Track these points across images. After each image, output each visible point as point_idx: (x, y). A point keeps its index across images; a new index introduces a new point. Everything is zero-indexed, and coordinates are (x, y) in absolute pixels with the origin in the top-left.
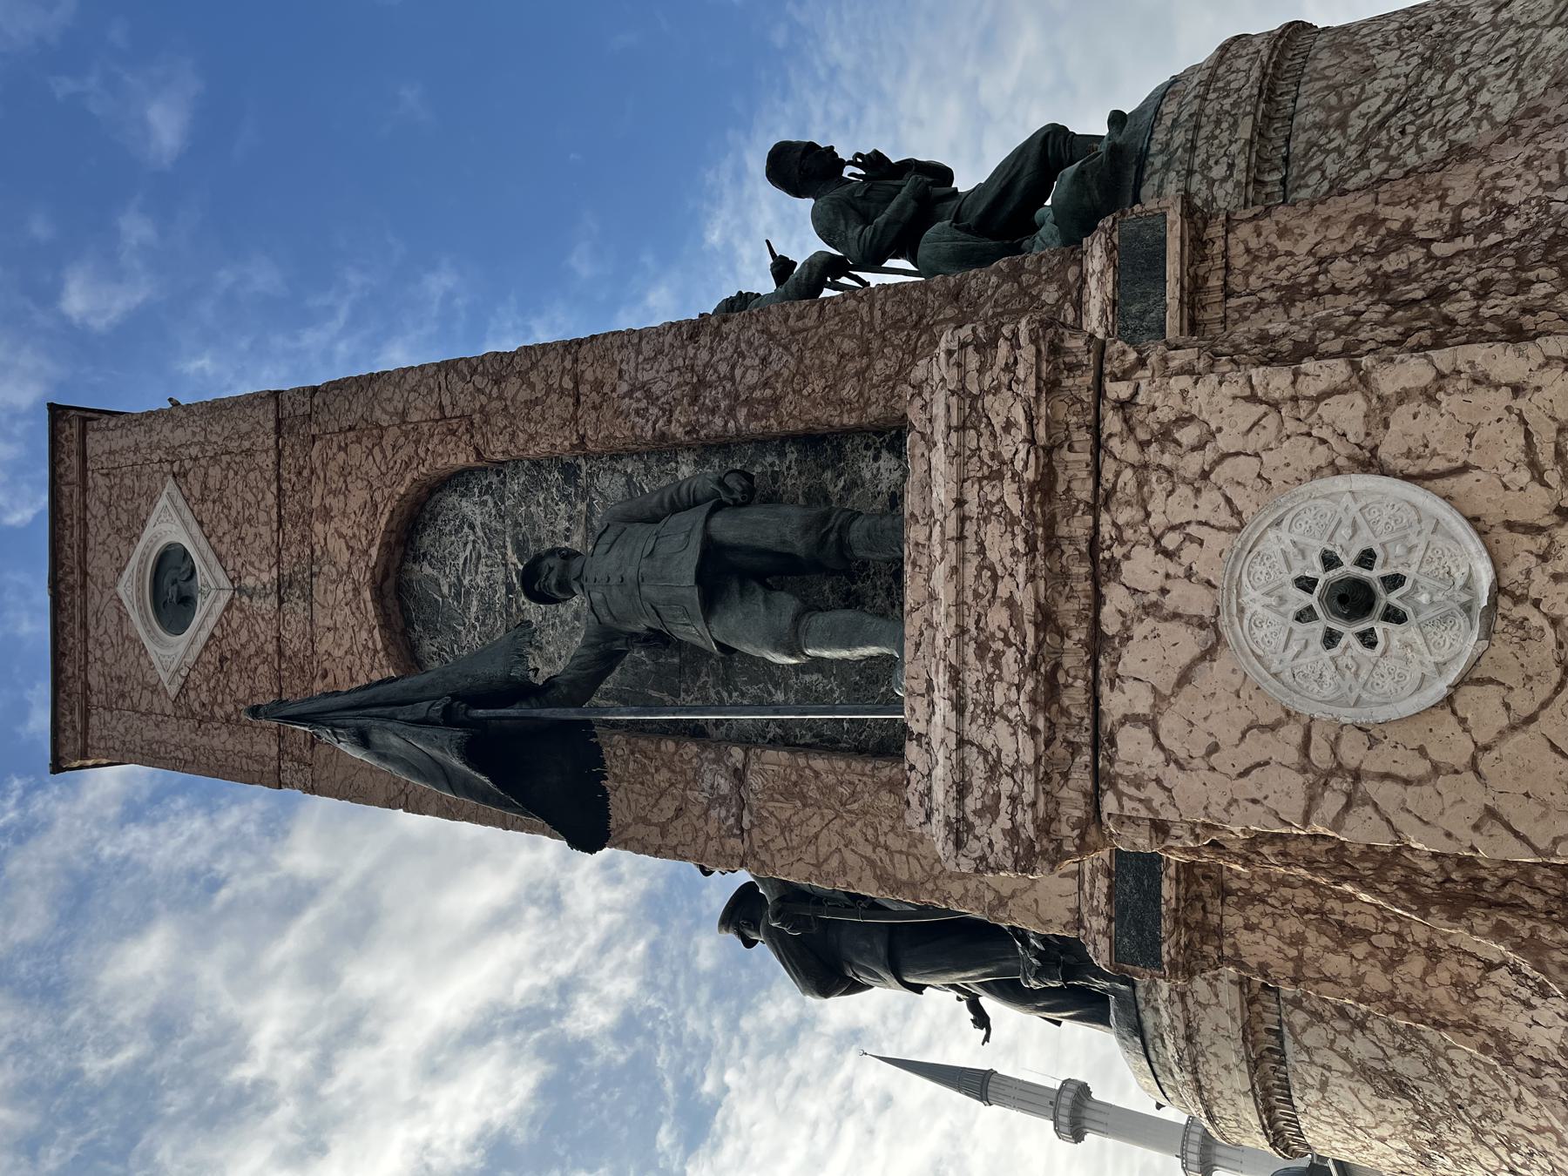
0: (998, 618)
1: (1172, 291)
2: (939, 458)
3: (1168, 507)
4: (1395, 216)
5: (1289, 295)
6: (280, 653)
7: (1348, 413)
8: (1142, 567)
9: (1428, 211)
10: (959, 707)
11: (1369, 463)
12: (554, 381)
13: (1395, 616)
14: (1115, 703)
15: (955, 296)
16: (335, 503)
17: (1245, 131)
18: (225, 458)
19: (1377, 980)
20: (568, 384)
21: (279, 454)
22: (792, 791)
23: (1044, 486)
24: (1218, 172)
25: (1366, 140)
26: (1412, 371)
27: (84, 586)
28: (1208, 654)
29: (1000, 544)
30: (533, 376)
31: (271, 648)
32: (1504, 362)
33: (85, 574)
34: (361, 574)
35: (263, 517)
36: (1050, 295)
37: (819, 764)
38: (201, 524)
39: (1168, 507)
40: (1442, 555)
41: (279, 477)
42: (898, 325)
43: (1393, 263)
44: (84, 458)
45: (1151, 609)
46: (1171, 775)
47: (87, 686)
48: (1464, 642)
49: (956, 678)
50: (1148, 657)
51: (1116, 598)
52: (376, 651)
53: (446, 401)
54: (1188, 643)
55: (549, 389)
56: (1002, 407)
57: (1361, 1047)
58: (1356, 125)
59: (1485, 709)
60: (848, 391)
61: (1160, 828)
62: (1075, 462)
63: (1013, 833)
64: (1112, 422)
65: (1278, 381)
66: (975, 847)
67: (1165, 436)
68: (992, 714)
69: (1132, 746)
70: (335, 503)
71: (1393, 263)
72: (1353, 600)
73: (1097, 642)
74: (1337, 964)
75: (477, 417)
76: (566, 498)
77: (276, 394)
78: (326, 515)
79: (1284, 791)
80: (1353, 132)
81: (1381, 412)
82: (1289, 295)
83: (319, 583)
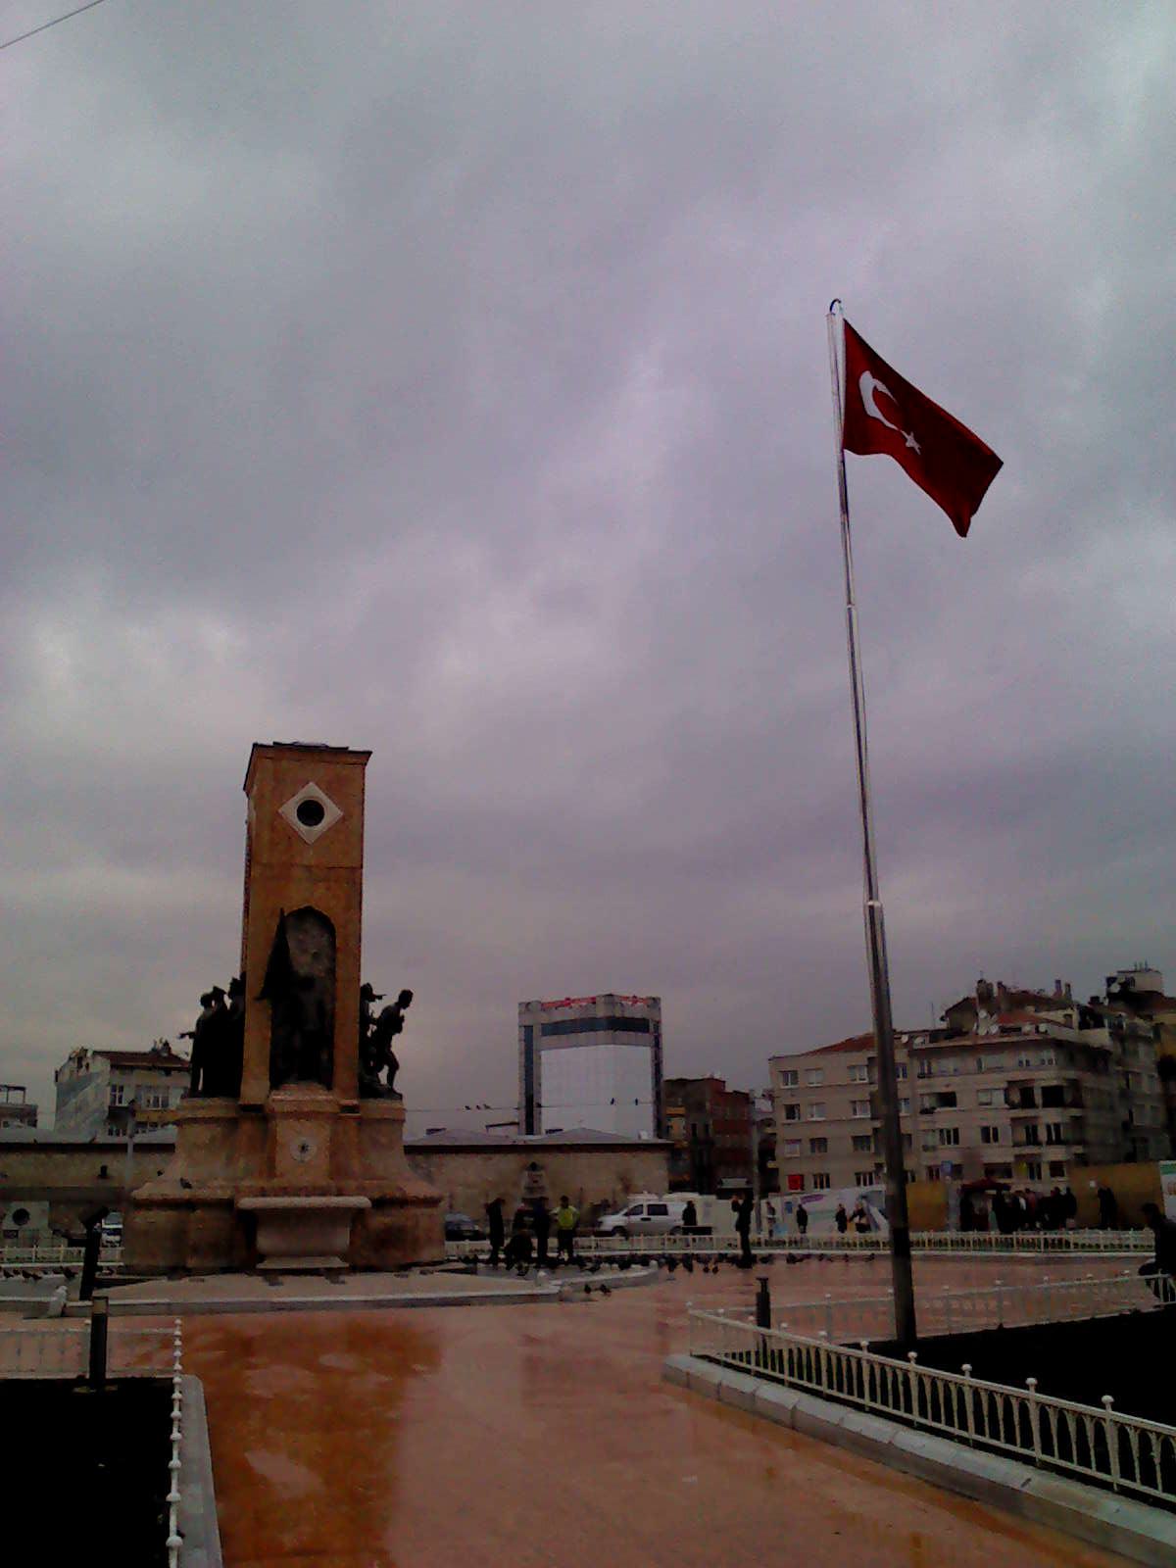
2: (324, 1097)
40: (307, 1157)
77: (362, 867)
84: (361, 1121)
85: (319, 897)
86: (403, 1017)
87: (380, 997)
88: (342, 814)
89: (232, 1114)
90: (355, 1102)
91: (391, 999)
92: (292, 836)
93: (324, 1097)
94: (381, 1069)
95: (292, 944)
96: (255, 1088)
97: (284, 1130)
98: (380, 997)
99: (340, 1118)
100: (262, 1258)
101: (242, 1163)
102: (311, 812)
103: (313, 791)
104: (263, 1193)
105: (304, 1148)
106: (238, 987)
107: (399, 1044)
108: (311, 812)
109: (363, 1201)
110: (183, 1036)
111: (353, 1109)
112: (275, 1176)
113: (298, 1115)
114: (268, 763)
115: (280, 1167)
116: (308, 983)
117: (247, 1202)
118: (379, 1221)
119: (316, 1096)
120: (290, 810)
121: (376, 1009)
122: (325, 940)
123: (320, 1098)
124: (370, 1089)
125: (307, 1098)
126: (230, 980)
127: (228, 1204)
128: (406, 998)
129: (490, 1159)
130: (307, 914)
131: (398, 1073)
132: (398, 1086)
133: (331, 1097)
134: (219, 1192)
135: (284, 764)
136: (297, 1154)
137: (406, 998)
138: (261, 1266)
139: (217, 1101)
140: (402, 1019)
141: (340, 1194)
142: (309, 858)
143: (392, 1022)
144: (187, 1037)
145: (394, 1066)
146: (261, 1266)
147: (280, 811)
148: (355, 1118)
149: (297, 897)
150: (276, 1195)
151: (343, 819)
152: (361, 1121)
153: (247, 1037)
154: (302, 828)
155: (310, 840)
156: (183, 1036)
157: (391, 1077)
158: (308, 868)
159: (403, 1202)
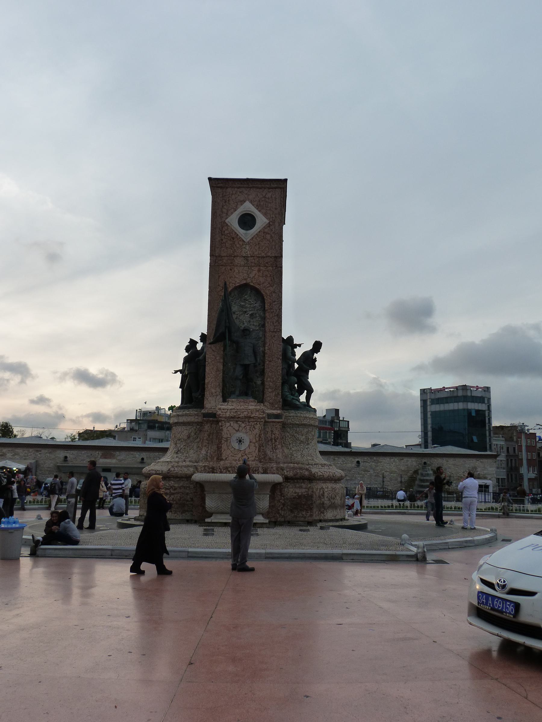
0: (239, 413)
1: (274, 420)
2: (254, 407)
3: (248, 427)
4: (278, 441)
5: (272, 431)
6: (235, 257)
7: (254, 441)
8: (243, 425)
9: (277, 443)
11: (250, 442)
14: (232, 423)
15: (278, 394)
16: (261, 274)
17: (297, 422)
18: (271, 240)
19: (205, 438)
20: (275, 330)
21: (271, 257)
22: (218, 370)
23: (250, 417)
24: (293, 420)
25: (293, 435)
26: (257, 445)
27: (248, 187)
29: (246, 413)
31: (235, 254)
32: (257, 451)
33: (251, 188)
34: (249, 281)
35: (260, 252)
36: (276, 406)
37: (221, 374)
39: (248, 427)
40: (243, 447)
42: (276, 386)
43: (273, 440)
44: (275, 188)
45: (240, 426)
47: (227, 188)
48: (237, 448)
50: (236, 426)
51: (240, 423)
53: (276, 303)
56: (257, 413)
57: (193, 434)
58: (295, 434)
59: (233, 449)
60: (269, 379)
61: (222, 426)
62: (252, 420)
65: (257, 436)
67: (254, 427)
68: (230, 412)
69: (228, 424)
70: (261, 274)
71: (273, 440)
72: (240, 441)
73: (237, 421)
74: (206, 435)
76: (259, 325)
78: (259, 271)
79: (225, 436)
80: (295, 434)
82: (272, 431)
83: (246, 268)
84: (284, 426)
85: (254, 276)
86: (316, 358)
87: (300, 345)
88: (268, 221)
89: (200, 419)
90: (279, 412)
91: (308, 346)
92: (234, 237)
93: (254, 407)
94: (302, 393)
95: (235, 308)
96: (213, 402)
97: (227, 429)
98: (300, 345)
99: (268, 422)
100: (210, 515)
101: (203, 452)
103: (248, 207)
104: (213, 470)
105: (240, 441)
106: (203, 337)
107: (313, 377)
108: (247, 221)
109: (277, 478)
110: (176, 372)
111: (278, 416)
112: (222, 460)
113: (235, 418)
114: (220, 190)
115: (226, 453)
116: (246, 332)
117: (198, 477)
118: (291, 491)
119: (250, 406)
120: (233, 220)
121: (299, 353)
122: (258, 305)
123: (251, 407)
124: (290, 404)
125: (242, 407)
127: (188, 477)
128: (317, 346)
129: (403, 459)
130: (244, 288)
132: (312, 403)
133: (259, 407)
134: (186, 469)
135: (229, 190)
136: (236, 445)
137: (317, 346)
138: (208, 520)
139: (192, 412)
140: (315, 360)
142: (247, 251)
143: (309, 361)
145: (310, 391)
146: (208, 520)
147: (227, 221)
148: (279, 422)
149: (238, 276)
150: (221, 472)
151: (269, 225)
152: (284, 426)
153: (207, 369)
154: (241, 232)
155: (247, 239)
156: (176, 372)
157: (308, 398)
158: (246, 258)
159: (311, 479)
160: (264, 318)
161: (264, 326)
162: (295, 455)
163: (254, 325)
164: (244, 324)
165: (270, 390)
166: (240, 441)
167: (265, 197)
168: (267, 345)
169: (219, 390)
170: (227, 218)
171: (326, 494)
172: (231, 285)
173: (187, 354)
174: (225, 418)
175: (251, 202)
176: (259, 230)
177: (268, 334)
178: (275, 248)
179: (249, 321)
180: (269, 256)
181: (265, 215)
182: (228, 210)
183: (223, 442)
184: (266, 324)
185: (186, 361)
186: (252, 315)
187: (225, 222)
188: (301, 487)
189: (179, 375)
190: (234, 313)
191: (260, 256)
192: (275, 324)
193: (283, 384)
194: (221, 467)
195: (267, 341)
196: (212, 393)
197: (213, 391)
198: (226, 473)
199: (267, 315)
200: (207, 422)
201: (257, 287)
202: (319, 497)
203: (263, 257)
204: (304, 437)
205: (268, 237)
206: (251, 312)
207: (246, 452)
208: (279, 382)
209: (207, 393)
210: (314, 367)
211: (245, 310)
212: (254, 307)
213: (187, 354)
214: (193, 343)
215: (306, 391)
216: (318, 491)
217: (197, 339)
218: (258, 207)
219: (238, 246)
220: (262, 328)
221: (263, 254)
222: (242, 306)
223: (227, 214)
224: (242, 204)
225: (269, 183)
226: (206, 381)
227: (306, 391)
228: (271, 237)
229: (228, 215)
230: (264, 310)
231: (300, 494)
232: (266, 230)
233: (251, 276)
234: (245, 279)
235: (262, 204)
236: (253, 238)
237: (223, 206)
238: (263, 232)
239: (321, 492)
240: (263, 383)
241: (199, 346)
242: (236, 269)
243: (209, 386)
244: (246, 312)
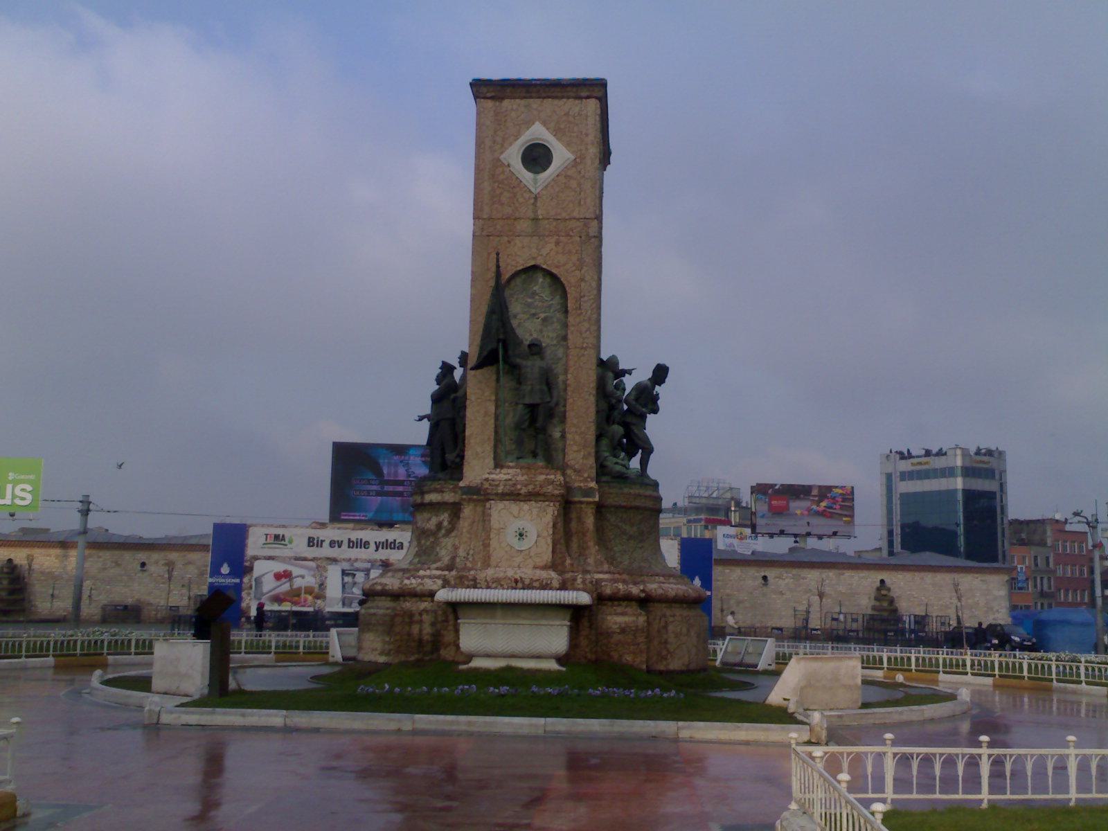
0: (519, 487)
6: (516, 219)
10: (506, 480)
11: (538, 536)
12: (586, 340)
13: (519, 539)
15: (589, 454)
21: (578, 219)
22: (486, 414)
24: (616, 499)
27: (539, 98)
28: (514, 516)
29: (530, 487)
30: (588, 332)
31: (517, 215)
37: (493, 421)
38: (558, 176)
40: (525, 545)
41: (570, 219)
44: (588, 97)
46: (497, 512)
49: (510, 480)
52: (517, 267)
53: (586, 298)
54: (516, 515)
55: (584, 339)
56: (550, 487)
58: (620, 524)
59: (508, 549)
61: (490, 509)
62: (542, 498)
63: (487, 489)
64: (547, 503)
66: (484, 483)
67: (545, 511)
74: (466, 524)
75: (579, 312)
78: (557, 243)
80: (620, 524)
81: (544, 538)
85: (548, 254)
87: (629, 372)
88: (572, 157)
91: (642, 374)
92: (515, 185)
98: (629, 372)
102: (537, 157)
103: (539, 132)
107: (654, 427)
108: (537, 157)
109: (584, 598)
110: (421, 419)
113: (513, 496)
114: (490, 104)
115: (497, 552)
116: (536, 349)
120: (513, 156)
121: (630, 383)
126: (459, 354)
128: (661, 373)
131: (652, 456)
132: (653, 471)
135: (506, 103)
137: (661, 373)
140: (656, 397)
141: (563, 587)
143: (647, 399)
144: (426, 420)
145: (648, 451)
147: (502, 157)
149: (519, 255)
150: (488, 587)
151: (575, 163)
154: (526, 176)
156: (421, 419)
157: (644, 462)
160: (565, 325)
161: (565, 338)
162: (619, 559)
163: (548, 338)
164: (531, 335)
165: (575, 448)
166: (521, 535)
167: (567, 114)
168: (571, 370)
169: (489, 448)
170: (502, 153)
171: (671, 628)
172: (509, 267)
173: (437, 387)
174: (497, 494)
175: (544, 123)
176: (556, 174)
177: (573, 352)
178: (585, 203)
179: (541, 331)
180: (574, 219)
181: (568, 145)
182: (504, 139)
183: (492, 535)
184: (570, 336)
185: (437, 399)
186: (545, 320)
187: (498, 160)
188: (623, 614)
189: (426, 425)
190: (515, 317)
191: (559, 217)
192: (584, 335)
193: (599, 437)
194: (488, 579)
195: (571, 363)
196: (477, 454)
197: (479, 450)
198: (496, 588)
199: (570, 319)
200: (470, 500)
201: (554, 271)
202: (659, 631)
203: (565, 220)
204: (635, 529)
205: (573, 184)
206: (542, 316)
207: (532, 554)
208: (591, 436)
209: (468, 454)
210: (655, 411)
211: (533, 311)
212: (550, 307)
213: (437, 387)
214: (447, 369)
215: (640, 451)
216: (657, 621)
217: (454, 362)
218: (557, 132)
219: (521, 200)
220: (562, 343)
221: (564, 215)
222: (529, 305)
223: (502, 145)
224: (528, 129)
225: (574, 89)
226: (467, 433)
227: (640, 451)
228: (579, 185)
229: (503, 148)
230: (566, 312)
231: (623, 625)
232: (569, 173)
233: (544, 252)
234: (534, 258)
235: (562, 126)
236: (546, 187)
237: (495, 132)
238: (564, 174)
239: (662, 624)
240: (563, 436)
241: (458, 373)
242: (517, 242)
243: (472, 441)
244: (534, 315)
